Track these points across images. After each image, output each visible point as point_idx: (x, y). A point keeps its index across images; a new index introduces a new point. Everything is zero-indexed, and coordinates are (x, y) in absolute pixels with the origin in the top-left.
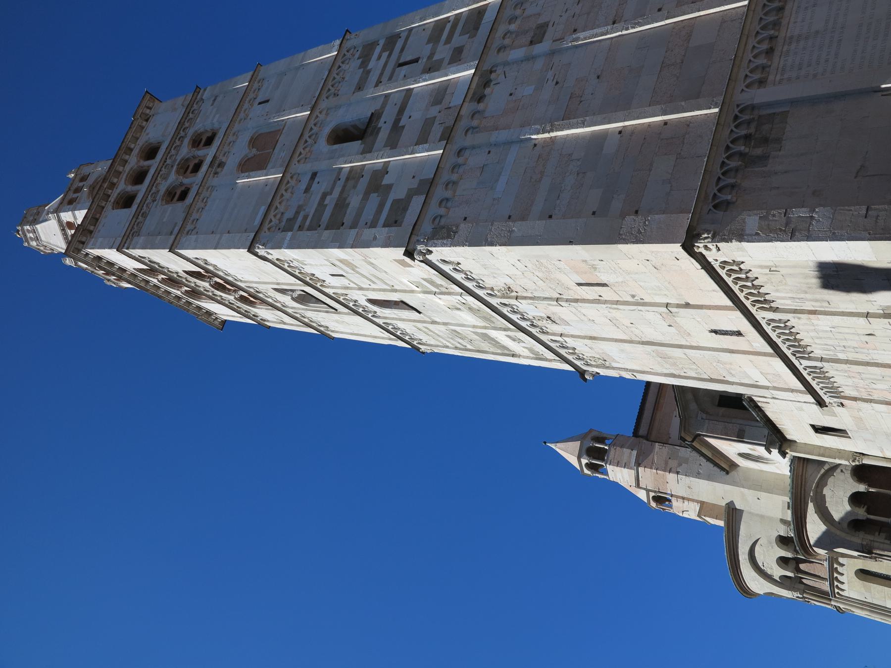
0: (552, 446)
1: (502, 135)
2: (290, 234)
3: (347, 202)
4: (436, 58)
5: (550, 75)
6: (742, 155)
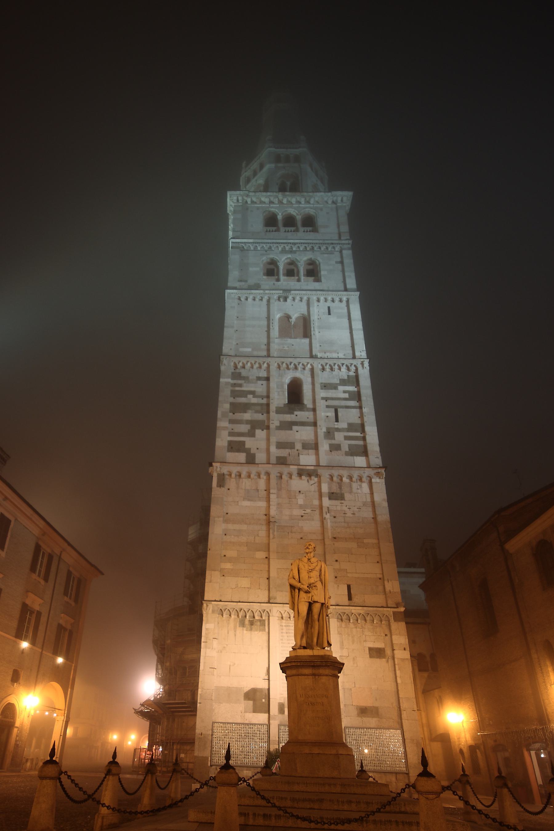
1: (273, 497)
2: (229, 380)
4: (336, 433)
5: (308, 511)
6: (246, 616)
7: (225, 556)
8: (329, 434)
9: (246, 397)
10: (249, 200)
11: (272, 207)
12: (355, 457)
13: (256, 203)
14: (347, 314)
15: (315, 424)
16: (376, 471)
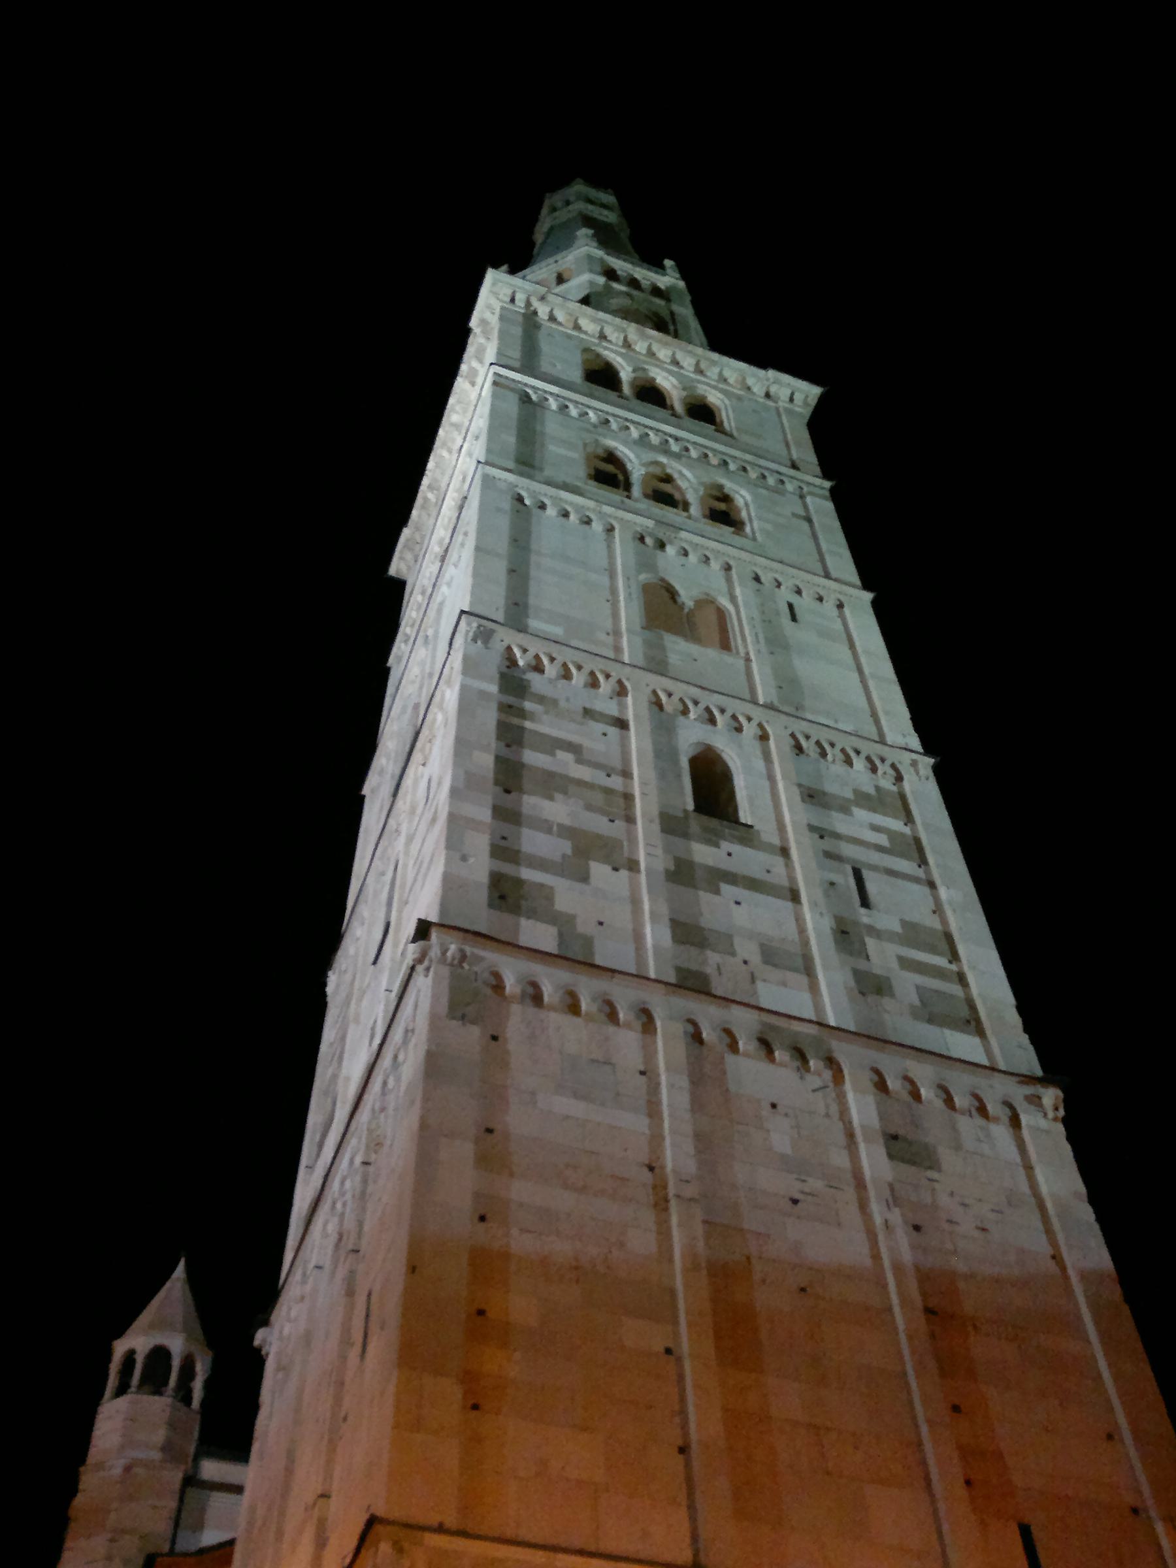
0: (180, 1271)
2: (494, 688)
3: (558, 796)
5: (816, 1184)
7: (481, 1313)
8: (846, 936)
9: (553, 754)
10: (543, 311)
11: (606, 348)
12: (947, 1032)
13: (560, 324)
14: (844, 636)
15: (795, 897)
16: (1029, 1090)
